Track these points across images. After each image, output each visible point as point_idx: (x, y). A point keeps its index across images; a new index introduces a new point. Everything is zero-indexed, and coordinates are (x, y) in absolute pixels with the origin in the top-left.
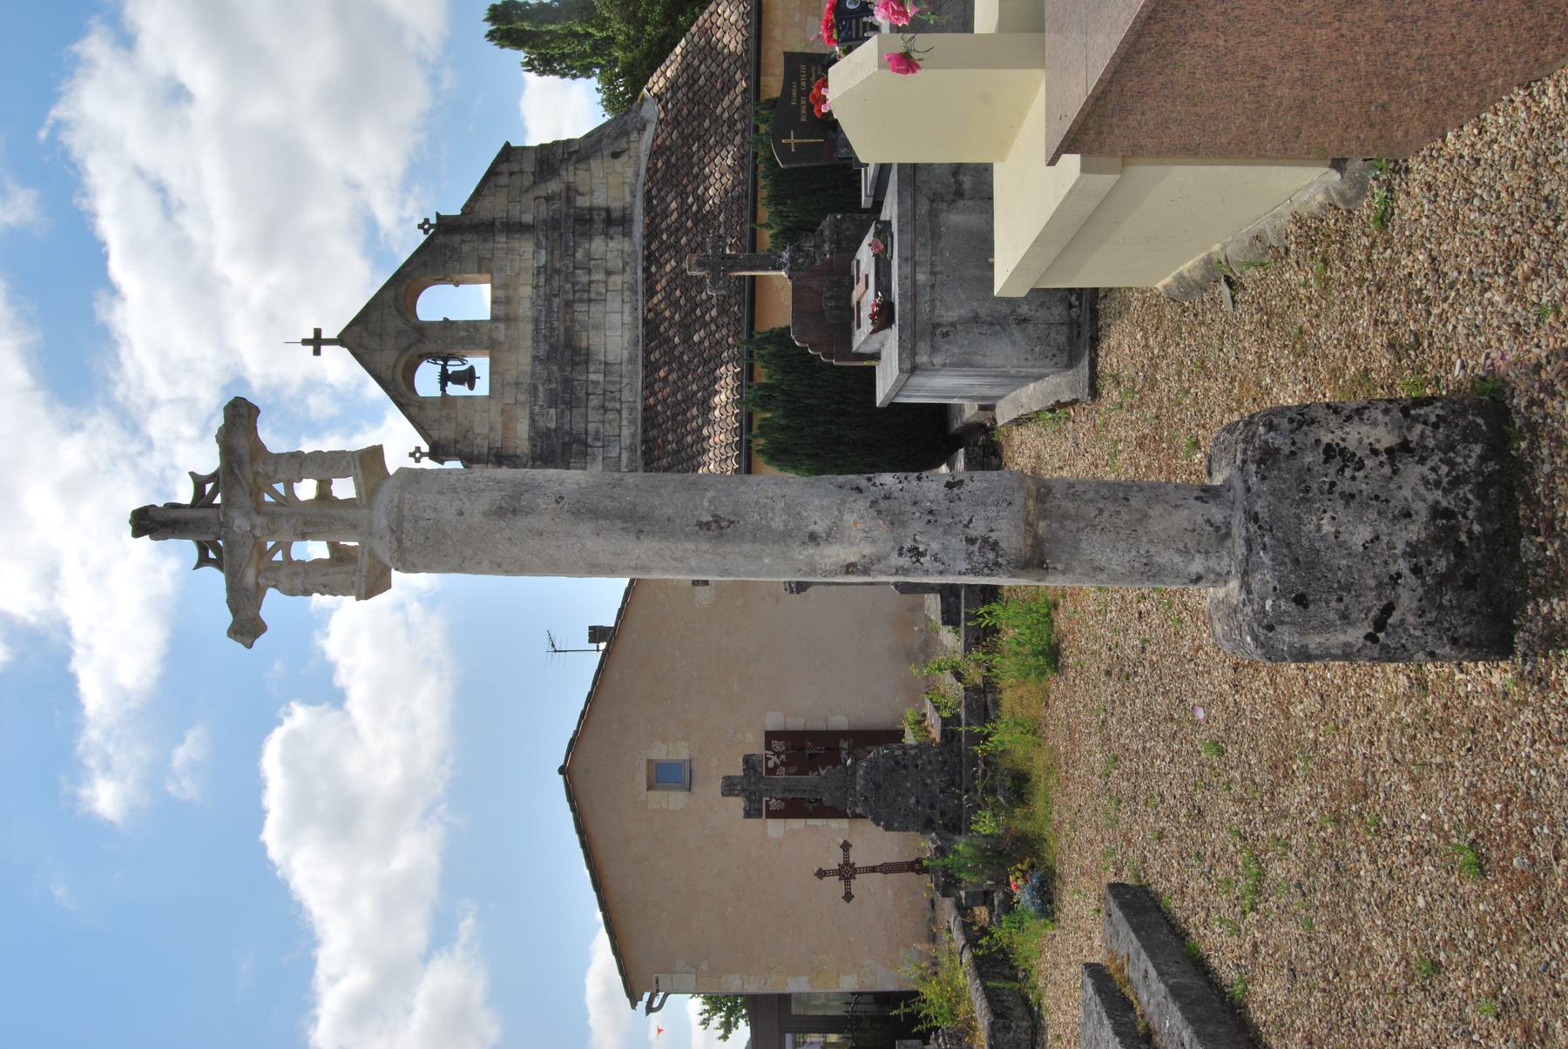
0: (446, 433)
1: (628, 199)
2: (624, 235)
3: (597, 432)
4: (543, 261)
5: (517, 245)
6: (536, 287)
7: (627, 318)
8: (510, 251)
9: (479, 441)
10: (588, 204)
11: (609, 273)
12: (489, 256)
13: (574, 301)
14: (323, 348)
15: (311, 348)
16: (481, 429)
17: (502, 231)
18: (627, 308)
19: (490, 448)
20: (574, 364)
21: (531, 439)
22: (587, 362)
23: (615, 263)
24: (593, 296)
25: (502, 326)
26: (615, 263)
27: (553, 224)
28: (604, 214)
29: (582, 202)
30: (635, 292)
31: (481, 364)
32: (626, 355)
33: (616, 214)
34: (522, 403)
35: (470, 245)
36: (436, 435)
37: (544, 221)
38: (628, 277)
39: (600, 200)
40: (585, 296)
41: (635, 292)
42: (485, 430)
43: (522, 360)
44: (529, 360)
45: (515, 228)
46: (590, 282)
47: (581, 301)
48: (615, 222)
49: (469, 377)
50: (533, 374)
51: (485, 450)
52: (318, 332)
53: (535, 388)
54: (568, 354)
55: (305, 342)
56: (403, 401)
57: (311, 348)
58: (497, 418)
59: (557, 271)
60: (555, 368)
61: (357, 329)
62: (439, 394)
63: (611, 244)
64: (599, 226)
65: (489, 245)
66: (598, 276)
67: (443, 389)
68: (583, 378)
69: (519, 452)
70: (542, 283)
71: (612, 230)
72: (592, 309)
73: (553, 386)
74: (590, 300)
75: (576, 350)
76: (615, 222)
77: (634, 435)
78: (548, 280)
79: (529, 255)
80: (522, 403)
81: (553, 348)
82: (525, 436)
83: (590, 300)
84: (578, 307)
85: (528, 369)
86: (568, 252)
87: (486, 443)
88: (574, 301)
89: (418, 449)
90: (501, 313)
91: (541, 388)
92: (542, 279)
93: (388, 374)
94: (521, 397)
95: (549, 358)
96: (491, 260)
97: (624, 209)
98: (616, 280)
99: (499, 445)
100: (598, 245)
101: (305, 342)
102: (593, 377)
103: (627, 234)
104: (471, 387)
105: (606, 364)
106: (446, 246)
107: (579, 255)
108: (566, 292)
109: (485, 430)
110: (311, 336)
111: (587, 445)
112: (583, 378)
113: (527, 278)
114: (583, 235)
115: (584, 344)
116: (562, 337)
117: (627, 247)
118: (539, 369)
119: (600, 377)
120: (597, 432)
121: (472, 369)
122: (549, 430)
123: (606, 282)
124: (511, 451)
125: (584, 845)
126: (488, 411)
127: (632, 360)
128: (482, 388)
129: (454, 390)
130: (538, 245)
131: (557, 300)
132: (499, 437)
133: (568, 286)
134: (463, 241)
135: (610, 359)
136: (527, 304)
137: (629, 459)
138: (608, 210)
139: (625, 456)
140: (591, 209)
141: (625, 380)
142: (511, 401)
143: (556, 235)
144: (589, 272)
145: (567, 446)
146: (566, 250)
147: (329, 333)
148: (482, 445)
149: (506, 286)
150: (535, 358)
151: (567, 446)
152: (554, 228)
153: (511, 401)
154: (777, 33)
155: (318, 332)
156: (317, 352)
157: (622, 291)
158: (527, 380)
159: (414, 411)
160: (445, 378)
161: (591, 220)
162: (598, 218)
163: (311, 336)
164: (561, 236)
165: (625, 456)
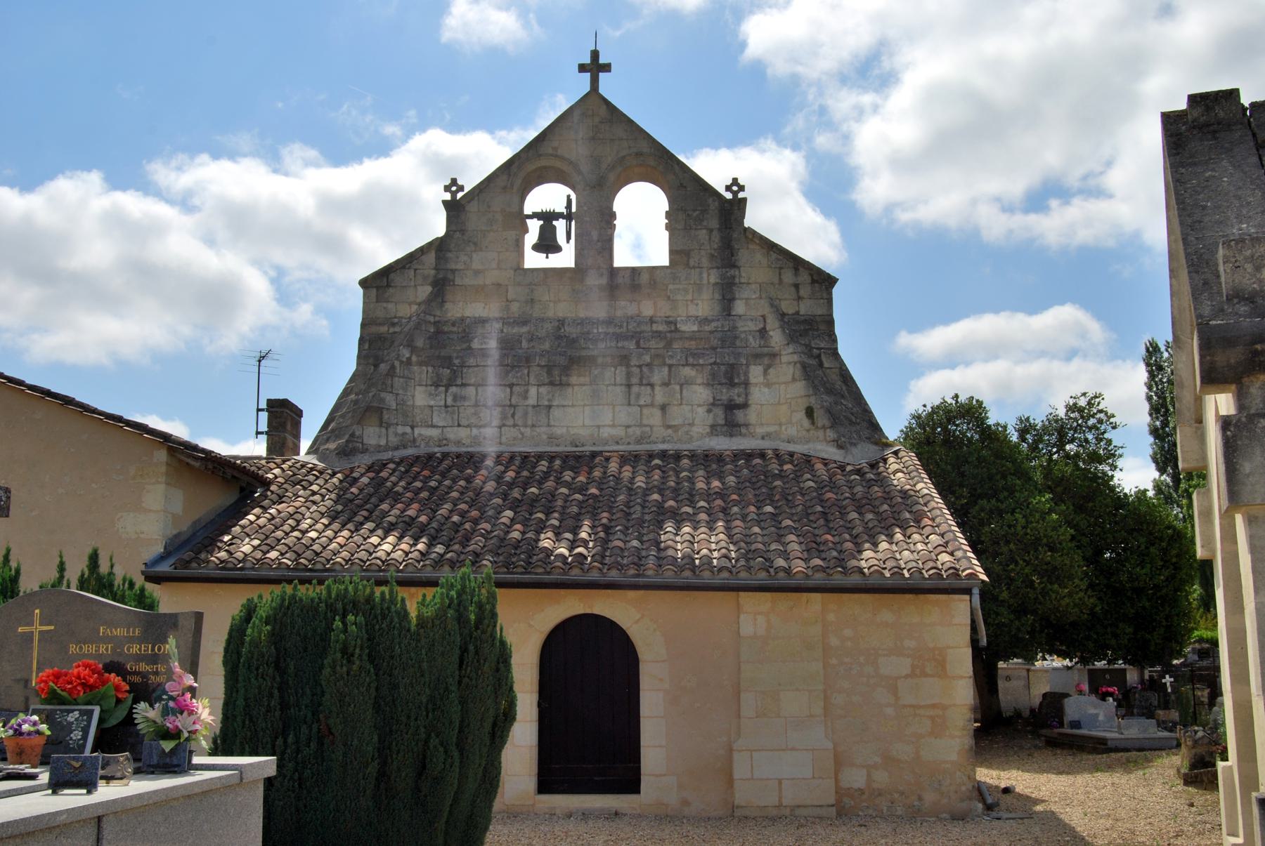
0: (474, 219)
1: (760, 431)
2: (713, 427)
3: (464, 398)
4: (683, 328)
5: (706, 295)
6: (652, 321)
7: (606, 432)
8: (699, 287)
9: (463, 258)
10: (752, 380)
11: (663, 408)
12: (692, 263)
13: (628, 366)
14: (587, 76)
15: (587, 60)
16: (477, 261)
17: (723, 277)
18: (620, 432)
19: (453, 271)
20: (549, 368)
21: (463, 319)
22: (552, 384)
23: (678, 415)
24: (635, 389)
25: (604, 281)
26: (678, 415)
27: (729, 339)
28: (740, 400)
29: (756, 373)
30: (638, 442)
31: (565, 258)
32: (559, 431)
33: (740, 416)
34: (507, 308)
35: (706, 239)
36: (472, 207)
37: (735, 328)
38: (660, 432)
39: (759, 395)
40: (635, 380)
41: (638, 442)
42: (476, 265)
43: (560, 307)
44: (561, 315)
45: (727, 293)
46: (652, 386)
47: (629, 375)
48: (731, 415)
49: (547, 244)
50: (542, 320)
51: (453, 266)
52: (607, 68)
53: (525, 323)
54: (562, 360)
55: (595, 55)
56: (514, 168)
57: (587, 60)
58: (492, 277)
59: (668, 345)
60: (547, 346)
61: (603, 110)
62: (528, 210)
63: (701, 411)
64: (725, 394)
65: (705, 262)
66: (660, 396)
67: (535, 215)
68: (532, 380)
69: (448, 306)
70: (655, 327)
71: (720, 412)
72: (618, 389)
73: (525, 344)
74: (629, 386)
75: (566, 370)
76: (731, 415)
77: (458, 443)
78: (658, 335)
79: (693, 311)
80: (507, 308)
81: (572, 342)
82: (468, 313)
83: (629, 386)
84: (621, 370)
85: (550, 314)
86: (691, 357)
87: (459, 266)
88: (628, 366)
89: (461, 188)
90: (620, 280)
91: (524, 329)
92: (661, 328)
93: (547, 148)
94: (515, 307)
95: (559, 338)
96: (687, 265)
97: (747, 425)
98: (654, 418)
99: (458, 281)
100: (701, 394)
101: (595, 55)
102: (533, 391)
103: (714, 430)
104: (537, 248)
105: (550, 407)
106: (704, 211)
107: (688, 372)
108: (640, 355)
109: (476, 265)
110: (602, 61)
111: (447, 387)
112: (532, 380)
113: (664, 310)
114: (714, 375)
115: (574, 379)
116: (584, 353)
117: (698, 430)
118: (548, 326)
119: (532, 401)
120: (464, 398)
121: (558, 249)
122: (470, 341)
123: (652, 405)
124: (449, 297)
125: (67, 401)
126: (499, 268)
127: (551, 437)
128: (533, 260)
129: (534, 226)
130: (706, 321)
131: (632, 345)
132: (467, 281)
133: (647, 359)
134: (711, 231)
135: (556, 413)
136: (631, 309)
137: (431, 438)
138: (745, 406)
139: (434, 433)
140: (746, 384)
141: (528, 431)
142: (511, 296)
143: (715, 342)
144: (666, 384)
145: (447, 362)
146: (694, 355)
147: (609, 86)
148: (457, 261)
149: (653, 284)
150: (562, 322)
151: (447, 362)
152: (723, 340)
153: (511, 296)
154: (886, 616)
155: (607, 68)
156: (582, 68)
157: (641, 425)
158: (536, 312)
159: (502, 181)
160: (547, 218)
161: (732, 385)
162: (736, 394)
163: (602, 61)
164: (714, 349)
165: (434, 433)
